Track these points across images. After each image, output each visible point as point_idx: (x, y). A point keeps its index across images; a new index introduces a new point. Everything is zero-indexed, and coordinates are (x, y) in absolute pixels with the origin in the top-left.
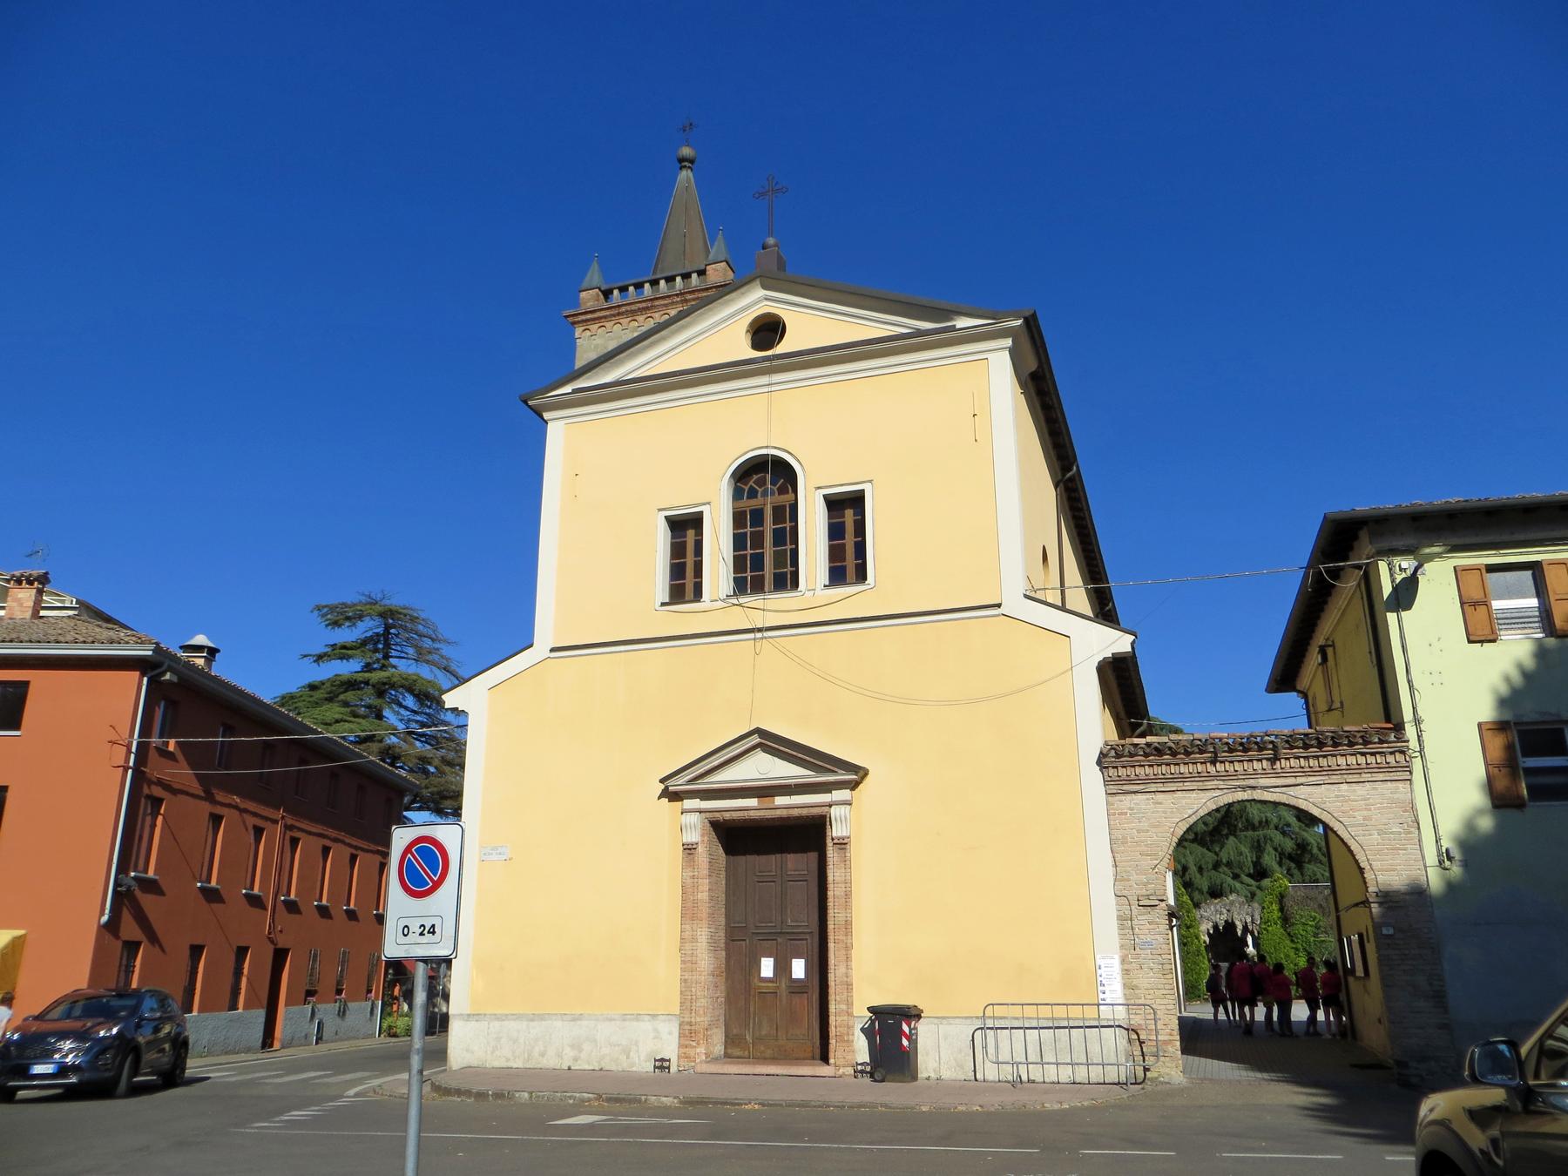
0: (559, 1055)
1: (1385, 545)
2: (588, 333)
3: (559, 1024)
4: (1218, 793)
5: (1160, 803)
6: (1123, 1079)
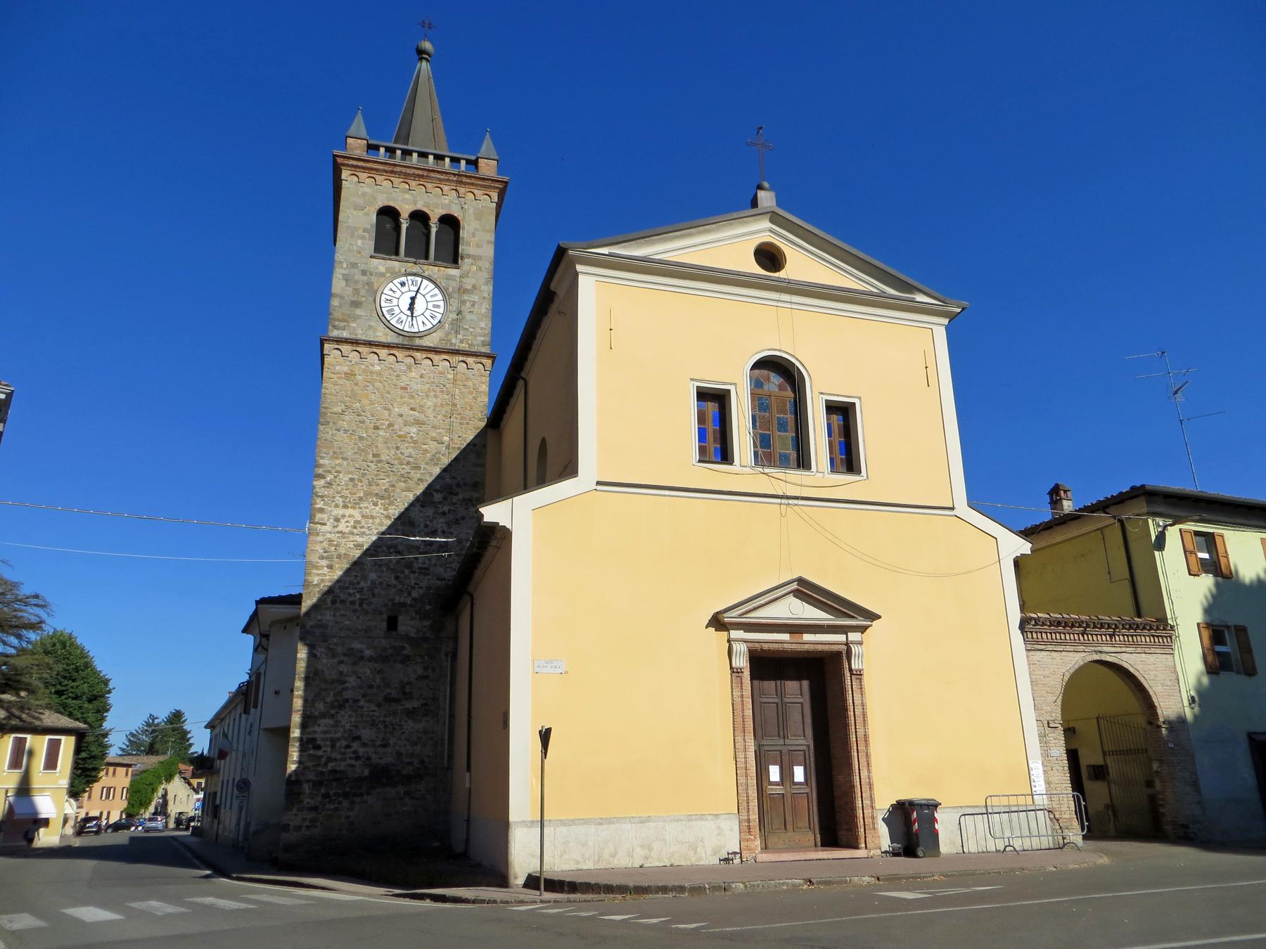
0: (630, 855)
1: (1152, 509)
2: (355, 179)
3: (627, 826)
4: (1084, 654)
5: (1054, 659)
6: (1052, 846)
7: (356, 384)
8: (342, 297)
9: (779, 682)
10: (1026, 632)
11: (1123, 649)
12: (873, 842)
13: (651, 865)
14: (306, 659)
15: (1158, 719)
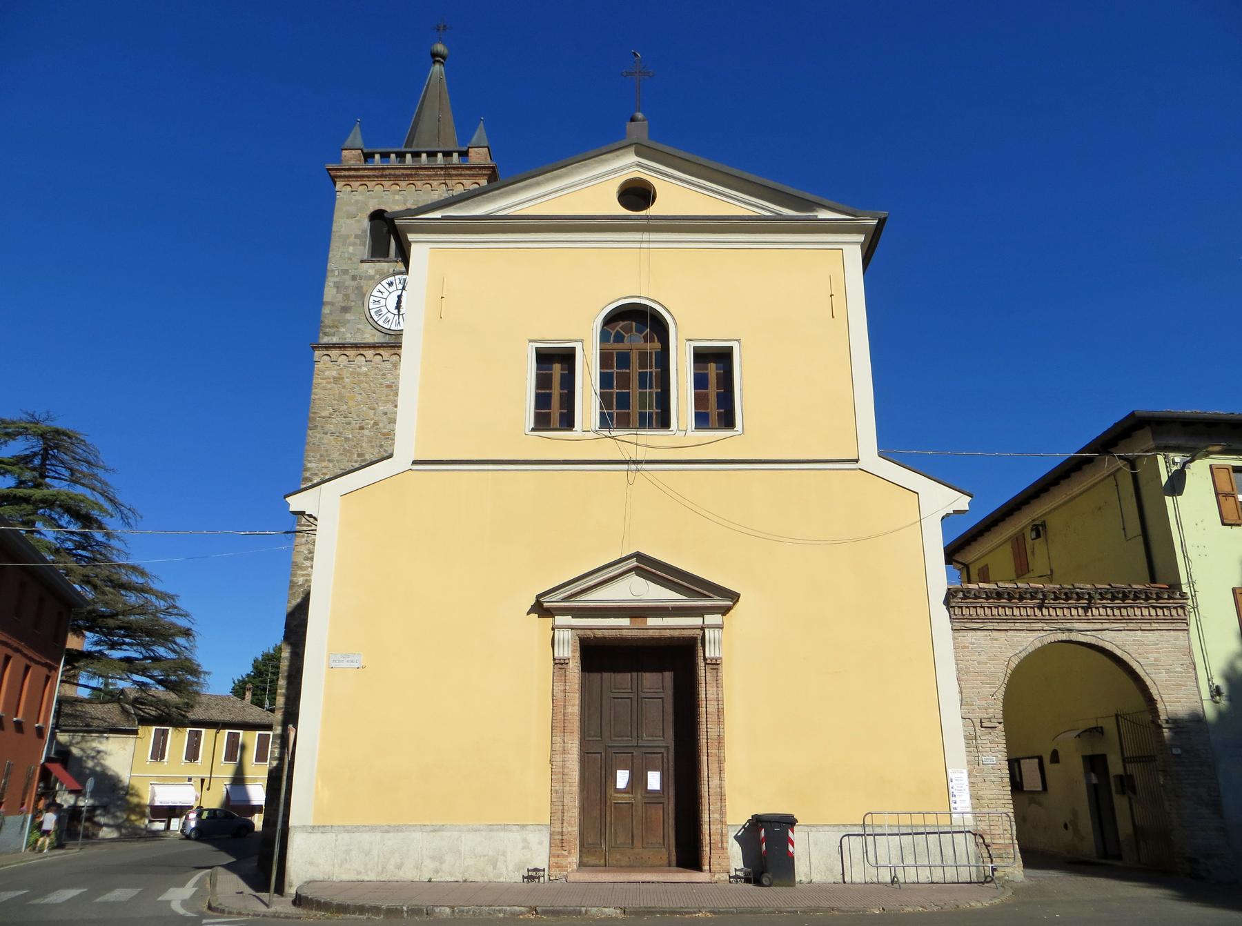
0: (418, 867)
1: (1163, 442)
2: (349, 188)
3: (418, 835)
4: (1043, 633)
5: (996, 640)
6: (974, 878)
7: (344, 387)
8: (332, 304)
9: (635, 674)
10: (953, 607)
11: (1106, 626)
12: (719, 864)
13: (441, 880)
14: (289, 658)
15: (1159, 716)
